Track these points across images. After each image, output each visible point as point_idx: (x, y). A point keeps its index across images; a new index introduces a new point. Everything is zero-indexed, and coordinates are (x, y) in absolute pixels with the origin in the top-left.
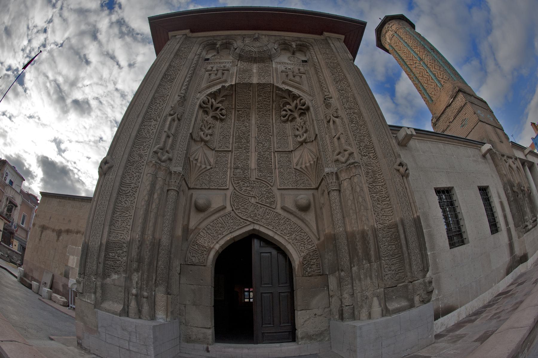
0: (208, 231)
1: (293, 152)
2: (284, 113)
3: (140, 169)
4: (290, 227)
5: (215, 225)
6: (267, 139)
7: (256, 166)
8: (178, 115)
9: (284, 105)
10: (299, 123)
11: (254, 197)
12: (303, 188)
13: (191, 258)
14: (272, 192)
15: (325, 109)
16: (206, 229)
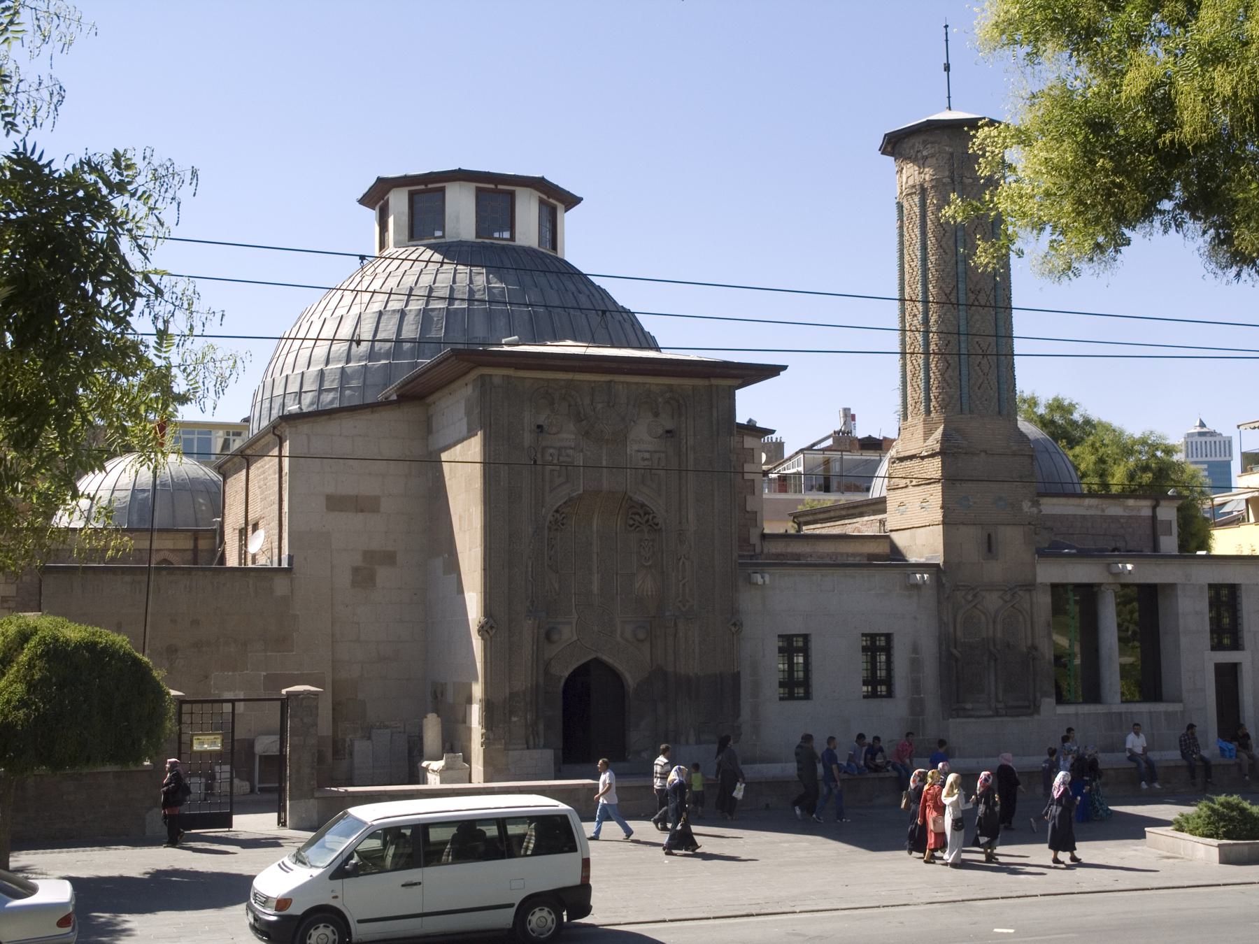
2: (631, 522)
9: (635, 514)
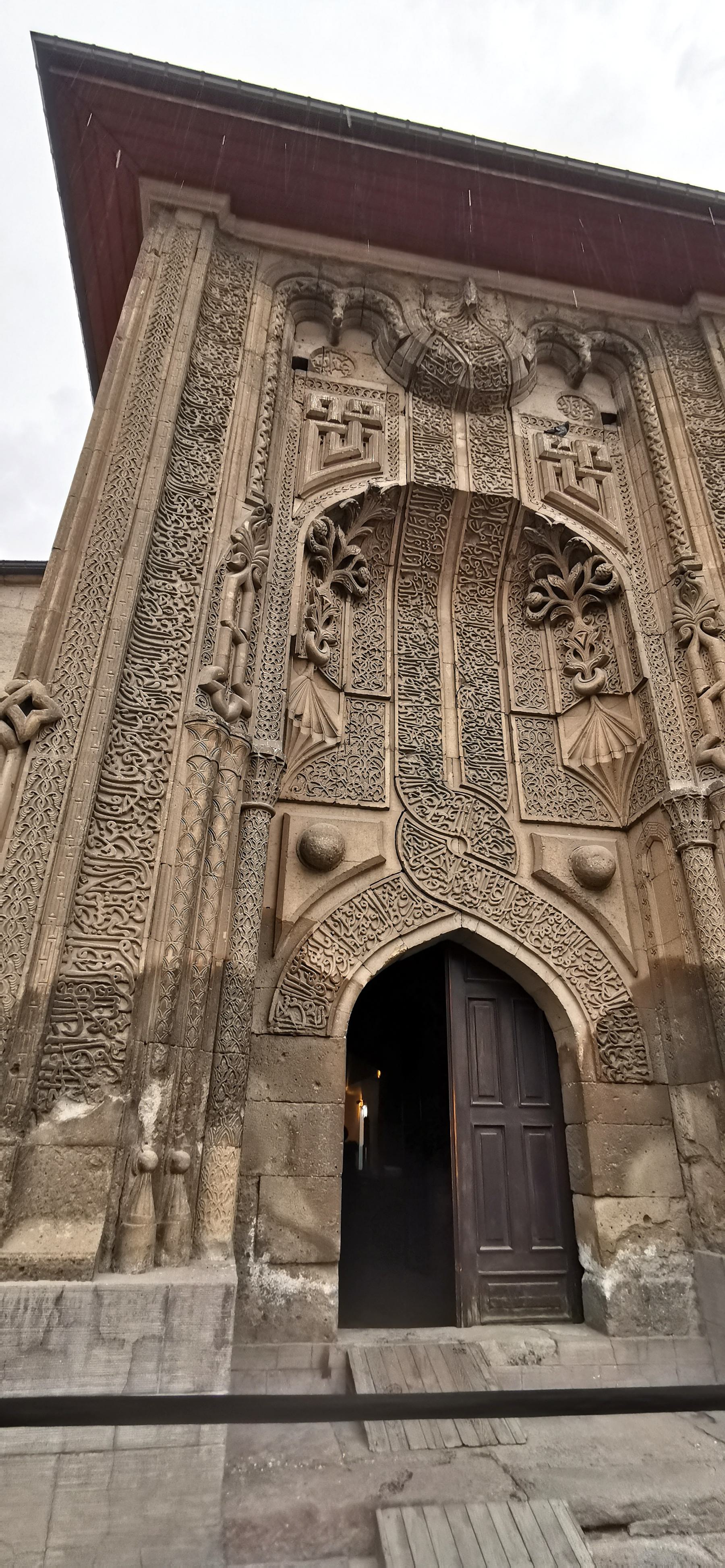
0: (337, 930)
1: (560, 720)
2: (537, 596)
3: (163, 740)
4: (557, 931)
5: (357, 912)
6: (488, 672)
7: (461, 749)
8: (254, 569)
10: (581, 636)
11: (459, 838)
12: (589, 823)
13: (286, 1014)
14: (505, 827)
15: (678, 602)
16: (330, 922)
